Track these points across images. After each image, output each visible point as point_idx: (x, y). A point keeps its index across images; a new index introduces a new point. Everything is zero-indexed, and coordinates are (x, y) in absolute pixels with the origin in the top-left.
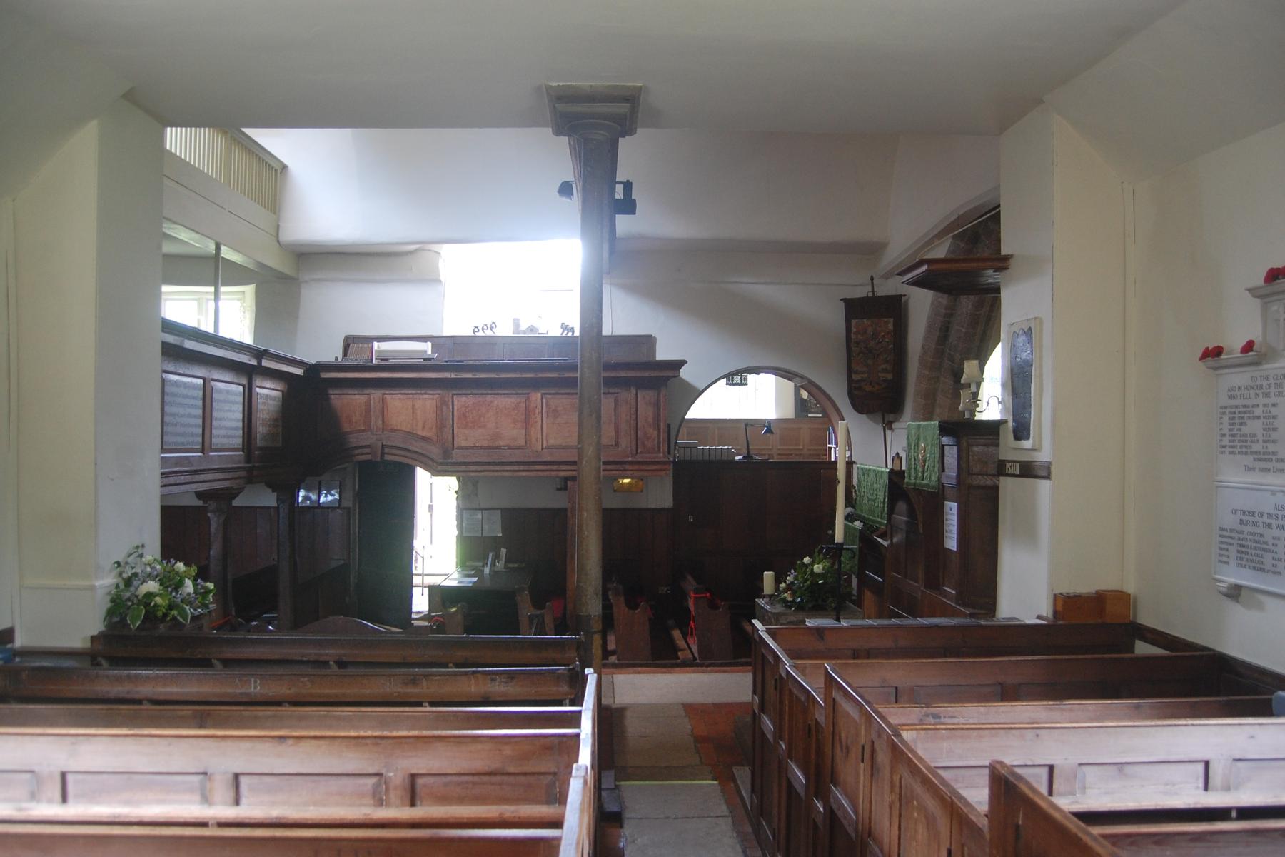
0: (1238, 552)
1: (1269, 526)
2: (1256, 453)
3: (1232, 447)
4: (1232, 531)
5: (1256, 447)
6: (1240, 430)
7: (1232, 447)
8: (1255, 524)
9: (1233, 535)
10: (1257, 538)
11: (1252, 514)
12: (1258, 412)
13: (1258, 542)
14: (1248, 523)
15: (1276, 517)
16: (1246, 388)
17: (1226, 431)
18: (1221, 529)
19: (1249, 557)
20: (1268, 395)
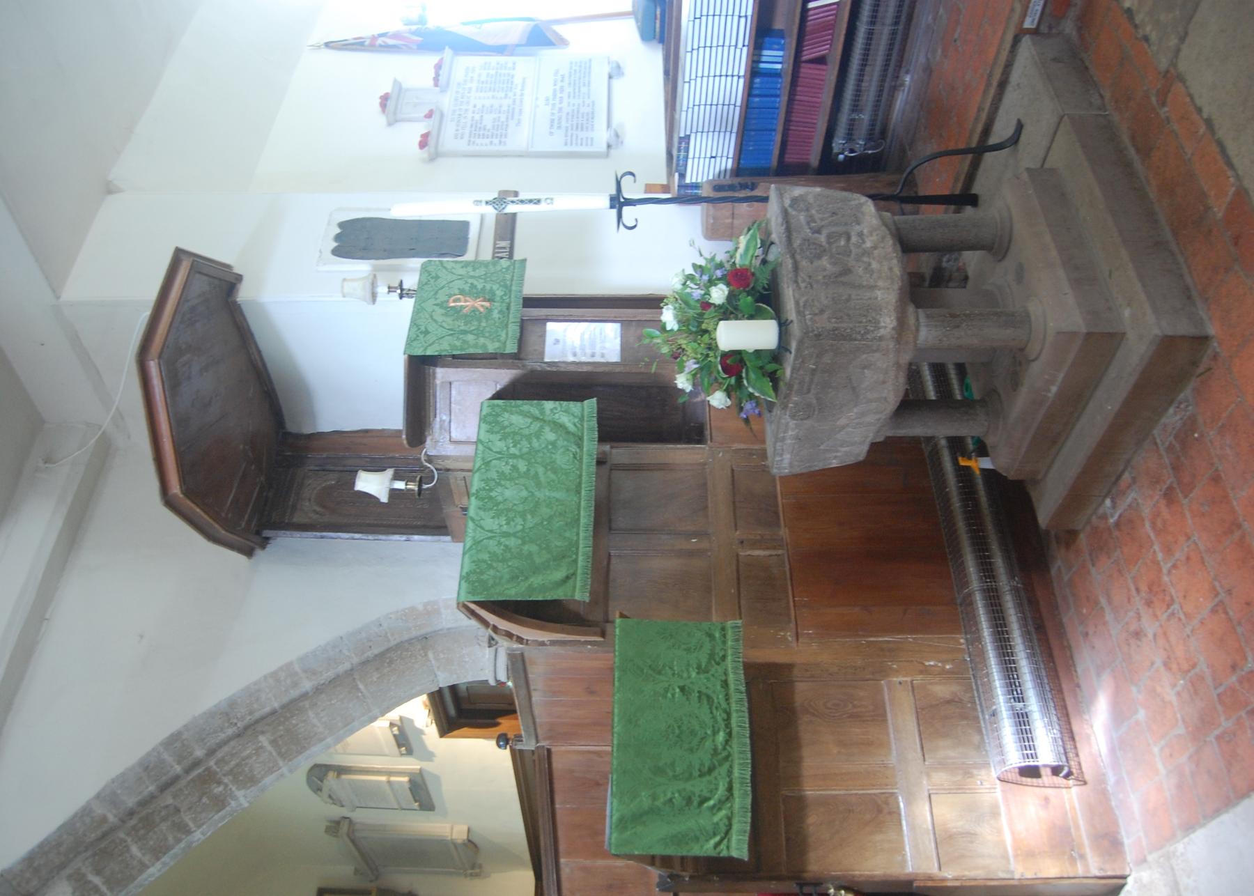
0: (582, 130)
1: (560, 109)
2: (507, 118)
3: (501, 136)
4: (566, 136)
5: (503, 118)
6: (489, 130)
7: (501, 136)
8: (560, 119)
9: (569, 134)
10: (570, 117)
11: (552, 121)
12: (477, 117)
13: (573, 116)
14: (559, 123)
15: (554, 105)
16: (458, 126)
17: (488, 141)
18: (566, 144)
19: (585, 122)
20: (466, 110)
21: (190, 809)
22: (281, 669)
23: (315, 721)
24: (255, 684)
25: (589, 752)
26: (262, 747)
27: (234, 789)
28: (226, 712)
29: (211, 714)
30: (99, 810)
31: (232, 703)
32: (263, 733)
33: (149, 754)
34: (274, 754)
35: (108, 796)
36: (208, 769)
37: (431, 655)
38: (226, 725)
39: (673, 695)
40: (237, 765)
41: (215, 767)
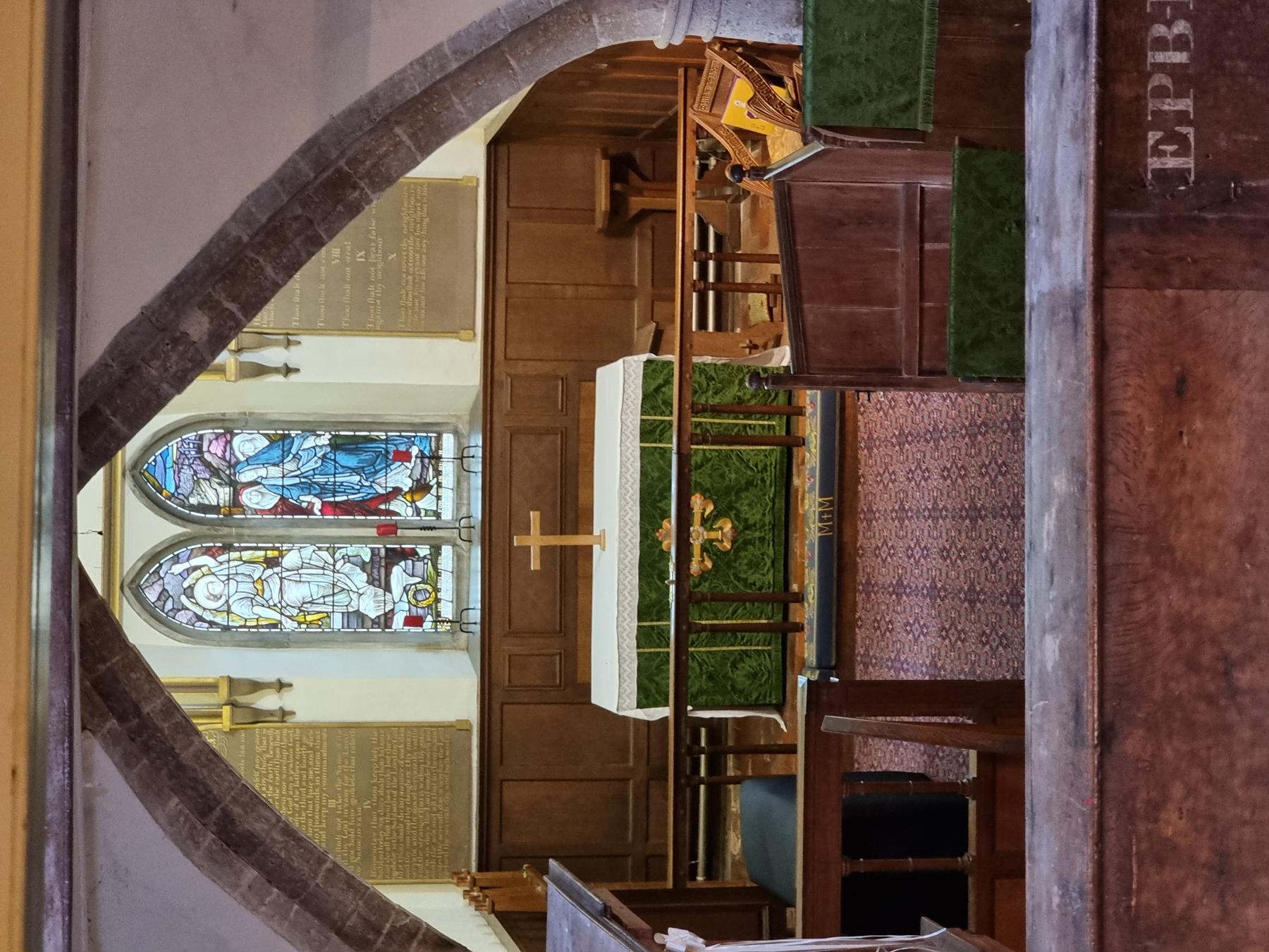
21: (324, 220)
22: (429, 53)
23: (460, 107)
24: (400, 72)
25: (833, 187)
26: (401, 142)
27: (369, 192)
28: (362, 110)
29: (350, 112)
30: (235, 231)
31: (373, 97)
32: (398, 123)
33: (285, 165)
34: (413, 148)
35: (242, 216)
36: (339, 171)
37: (595, 21)
38: (366, 122)
39: (1010, 229)
40: (375, 166)
41: (346, 168)
